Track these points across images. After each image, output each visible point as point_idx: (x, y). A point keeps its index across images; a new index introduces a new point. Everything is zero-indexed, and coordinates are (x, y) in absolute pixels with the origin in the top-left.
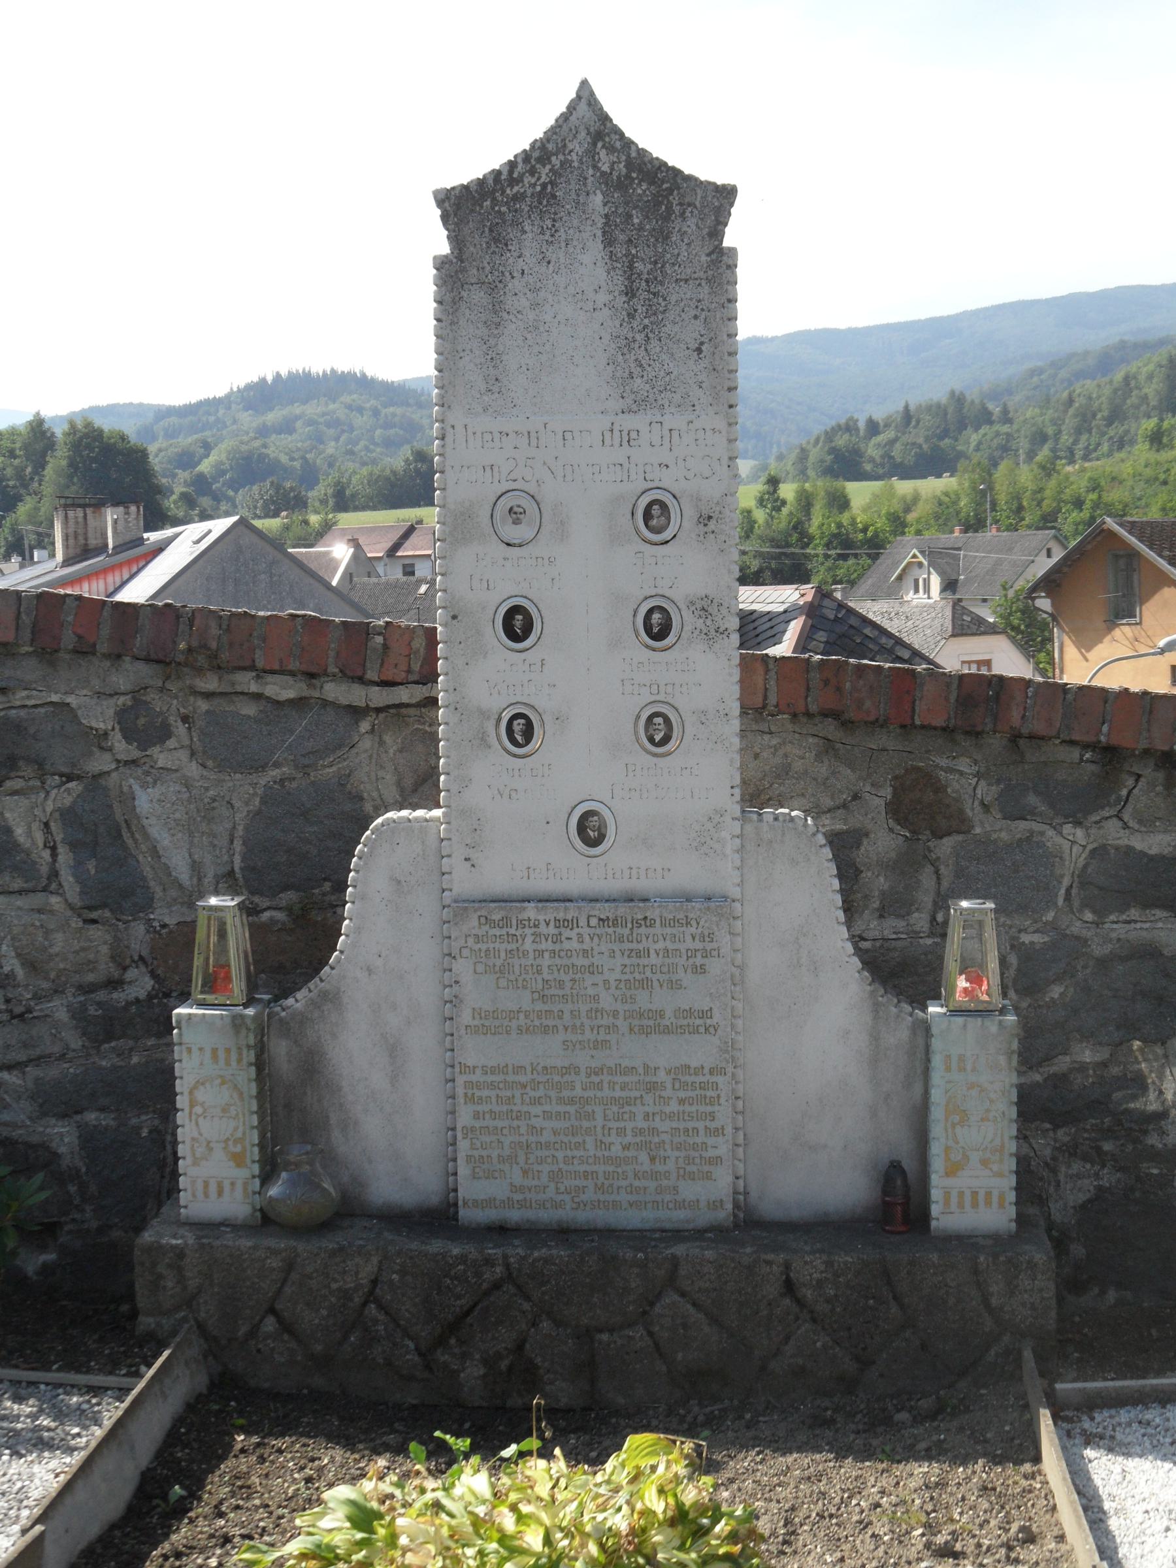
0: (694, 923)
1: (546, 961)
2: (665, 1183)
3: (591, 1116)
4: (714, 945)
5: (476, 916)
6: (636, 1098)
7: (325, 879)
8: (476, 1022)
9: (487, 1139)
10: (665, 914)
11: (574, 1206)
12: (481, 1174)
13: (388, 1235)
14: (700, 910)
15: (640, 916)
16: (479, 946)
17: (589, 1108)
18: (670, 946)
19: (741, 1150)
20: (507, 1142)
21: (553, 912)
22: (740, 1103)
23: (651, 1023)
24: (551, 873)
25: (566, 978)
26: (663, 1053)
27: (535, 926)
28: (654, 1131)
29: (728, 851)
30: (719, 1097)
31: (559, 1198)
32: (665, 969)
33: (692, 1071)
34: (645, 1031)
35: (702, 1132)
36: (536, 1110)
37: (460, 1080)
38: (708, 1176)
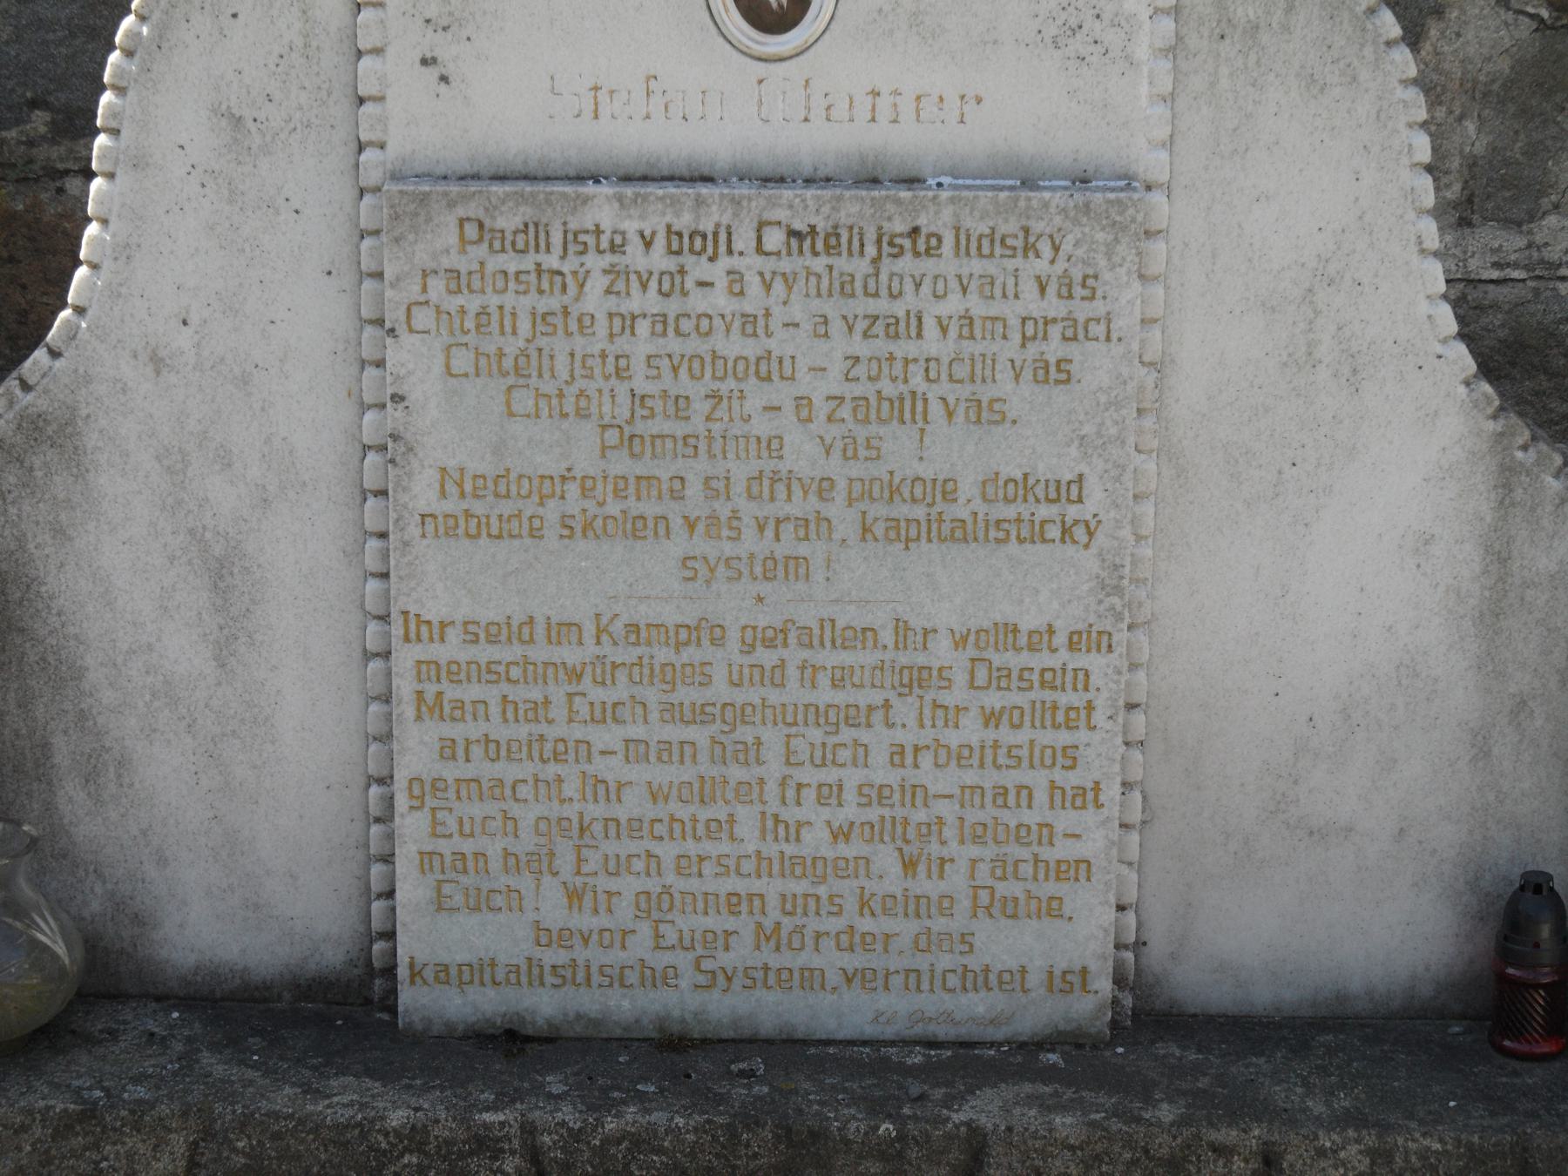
0: (1045, 248)
1: (642, 344)
2: (939, 924)
3: (751, 753)
4: (1099, 308)
5: (451, 220)
6: (871, 708)
7: (34, 104)
8: (450, 506)
9: (477, 810)
10: (968, 223)
11: (702, 979)
12: (459, 899)
13: (213, 1064)
14: (1063, 211)
15: (900, 226)
16: (460, 300)
17: (746, 734)
18: (978, 308)
19: (1135, 837)
20: (527, 815)
21: (661, 212)
22: (1139, 718)
23: (920, 512)
24: (657, 101)
25: (696, 390)
26: (949, 592)
27: (614, 248)
28: (914, 793)
29: (1142, 52)
30: (1090, 707)
31: (662, 960)
32: (961, 371)
33: (1023, 640)
34: (903, 534)
35: (1041, 797)
36: (607, 737)
37: (406, 657)
38: (1053, 909)
